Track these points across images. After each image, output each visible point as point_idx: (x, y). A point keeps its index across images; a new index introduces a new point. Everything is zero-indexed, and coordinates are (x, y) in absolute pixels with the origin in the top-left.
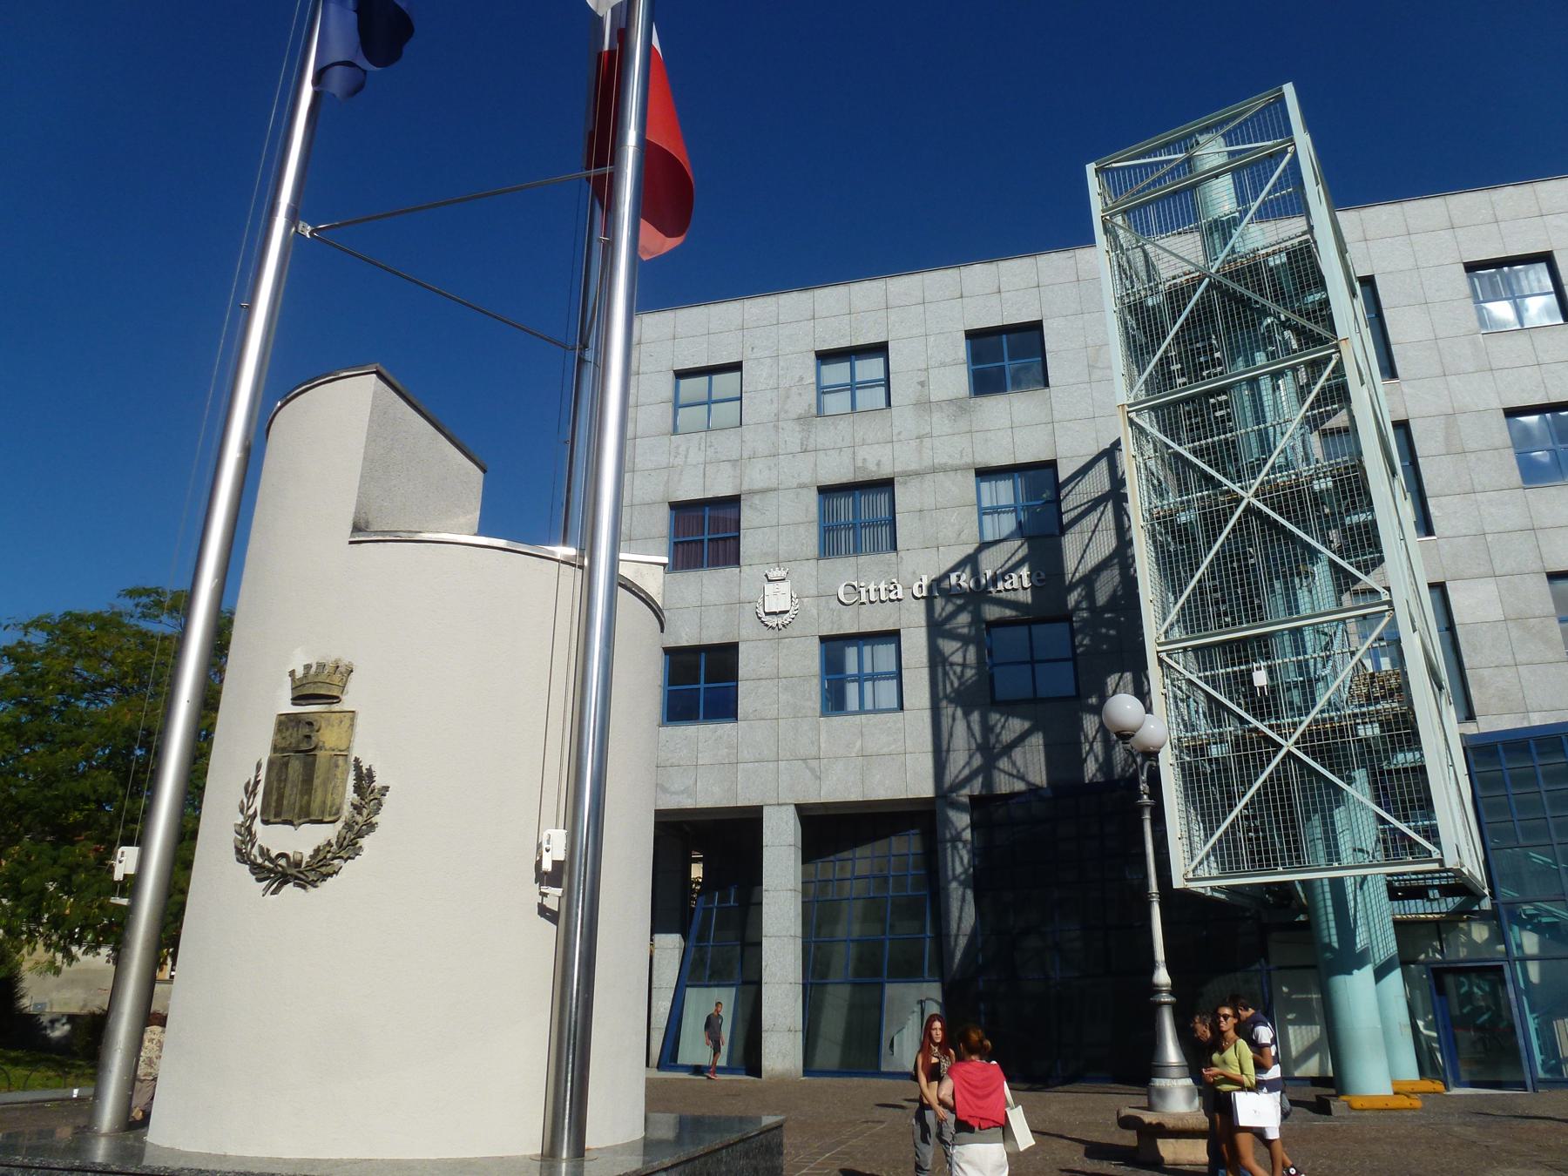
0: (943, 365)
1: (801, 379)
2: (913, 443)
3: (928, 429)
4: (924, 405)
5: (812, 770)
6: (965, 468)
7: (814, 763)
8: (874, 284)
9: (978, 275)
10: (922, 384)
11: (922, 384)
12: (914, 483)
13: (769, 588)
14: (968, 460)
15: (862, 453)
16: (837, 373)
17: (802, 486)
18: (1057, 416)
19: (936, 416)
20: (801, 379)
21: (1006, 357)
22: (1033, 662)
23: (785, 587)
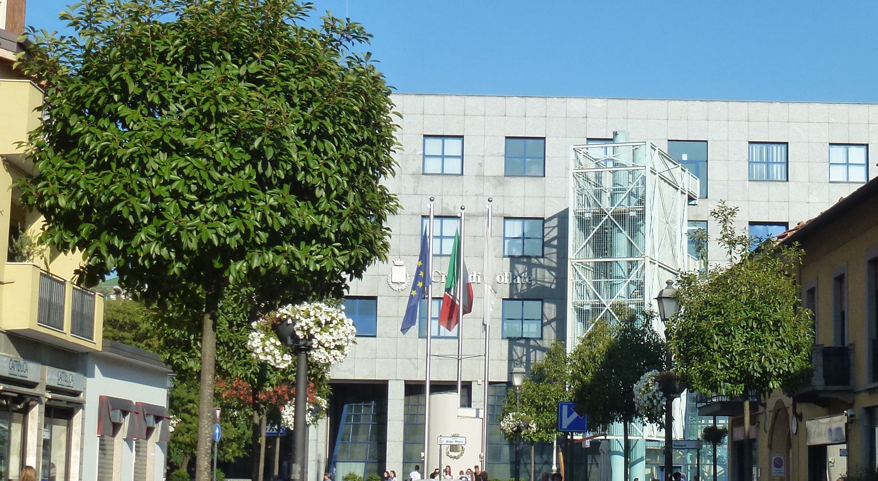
0: (492, 155)
1: (415, 150)
2: (474, 198)
3: (482, 191)
4: (481, 177)
5: (414, 364)
6: (499, 216)
7: (415, 361)
8: (458, 98)
9: (515, 103)
10: (480, 164)
11: (480, 164)
12: (472, 220)
13: (395, 268)
14: (500, 212)
15: (446, 200)
16: (434, 146)
17: (413, 214)
18: (547, 194)
19: (487, 184)
20: (415, 150)
21: (525, 154)
22: (522, 320)
23: (403, 269)
